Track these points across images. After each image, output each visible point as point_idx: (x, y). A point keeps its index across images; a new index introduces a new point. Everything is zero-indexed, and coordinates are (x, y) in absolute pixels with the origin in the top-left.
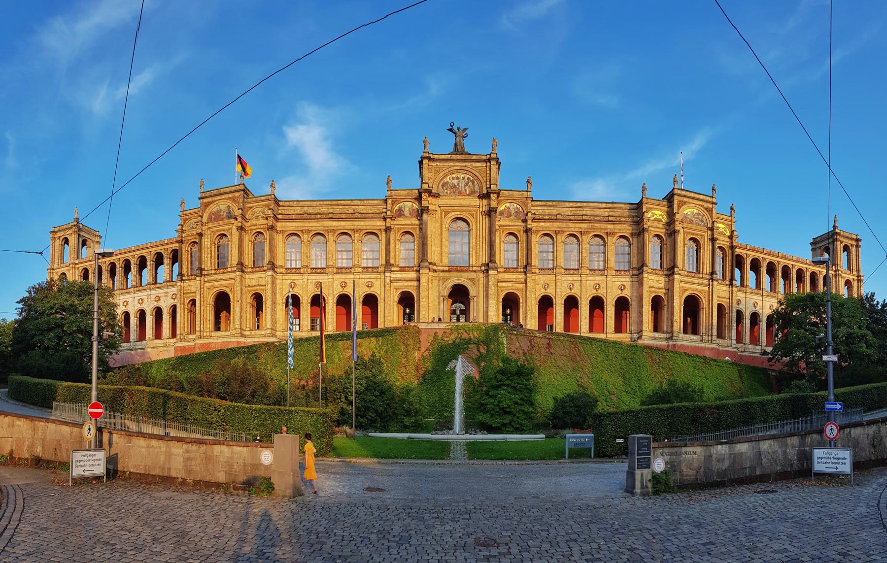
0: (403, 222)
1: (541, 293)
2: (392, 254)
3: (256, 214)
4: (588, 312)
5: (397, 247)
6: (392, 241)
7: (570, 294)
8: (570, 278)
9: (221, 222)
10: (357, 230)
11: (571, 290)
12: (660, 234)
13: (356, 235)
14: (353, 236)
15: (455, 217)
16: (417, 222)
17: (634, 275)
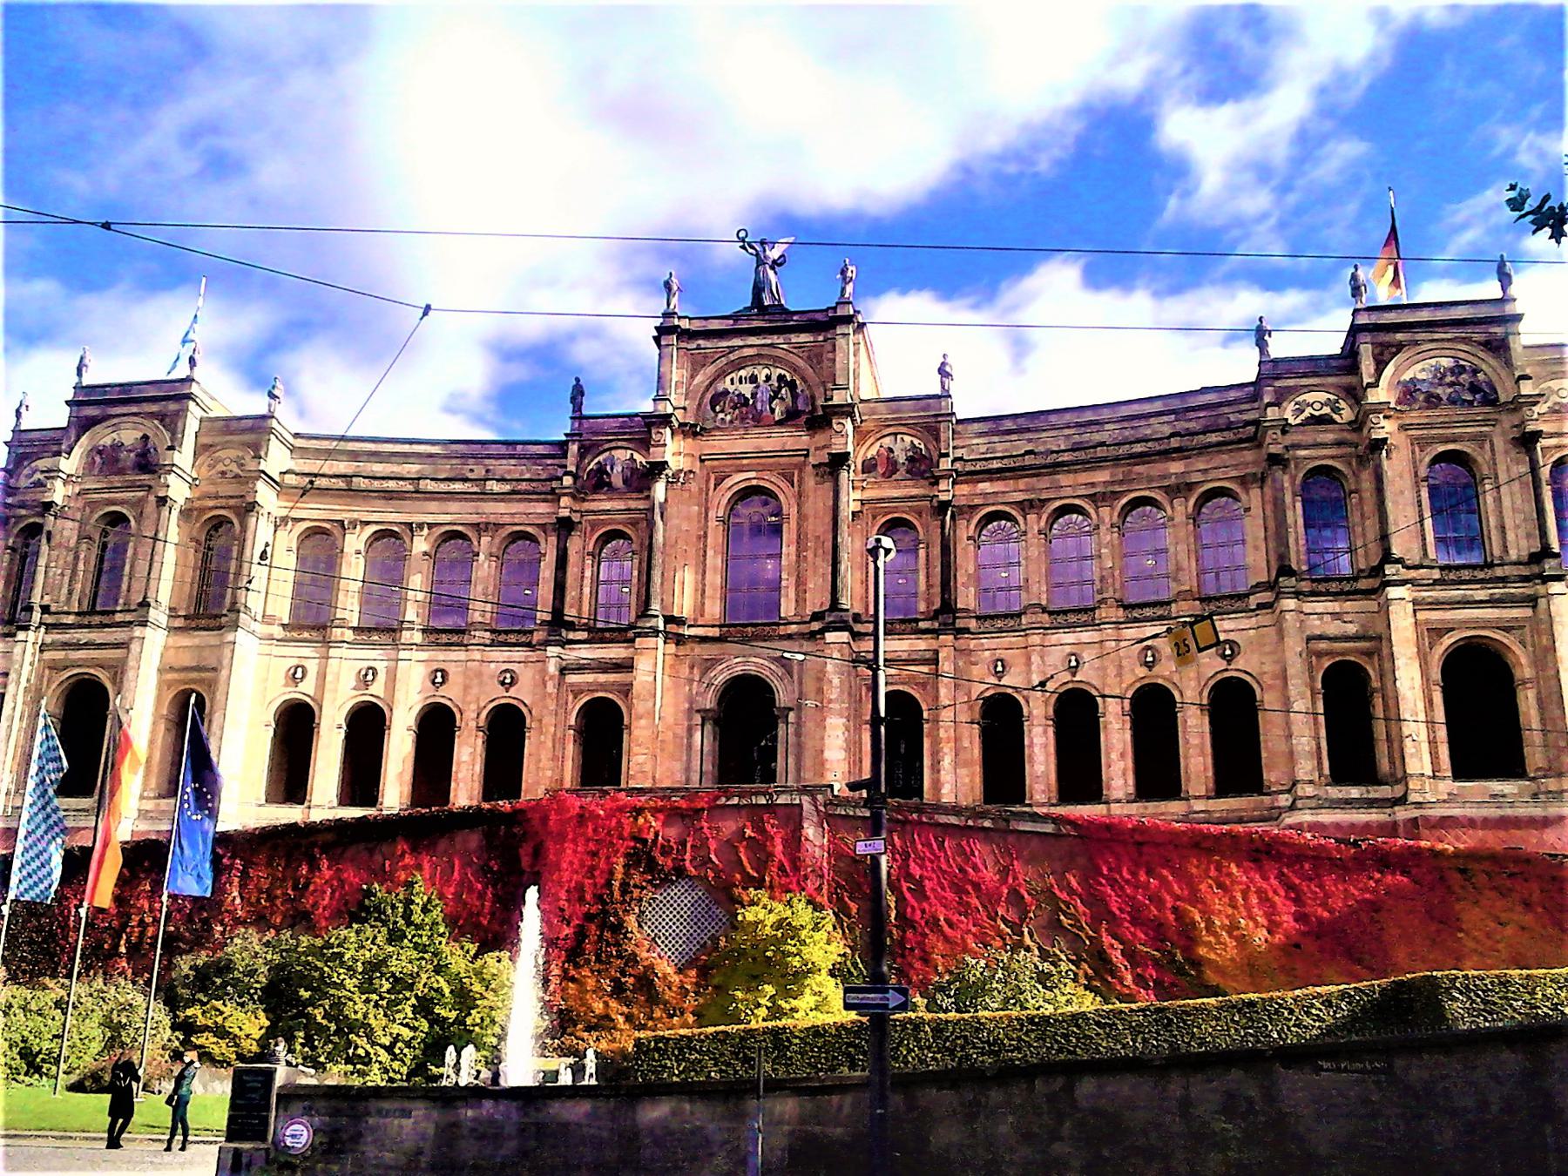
0: (607, 505)
1: (983, 684)
2: (571, 594)
3: (220, 467)
4: (1128, 735)
5: (588, 573)
6: (573, 557)
7: (1070, 686)
8: (1070, 638)
9: (116, 478)
10: (487, 524)
11: (1074, 675)
12: (1330, 462)
13: (485, 540)
14: (476, 543)
15: (742, 485)
16: (641, 505)
17: (1261, 606)
